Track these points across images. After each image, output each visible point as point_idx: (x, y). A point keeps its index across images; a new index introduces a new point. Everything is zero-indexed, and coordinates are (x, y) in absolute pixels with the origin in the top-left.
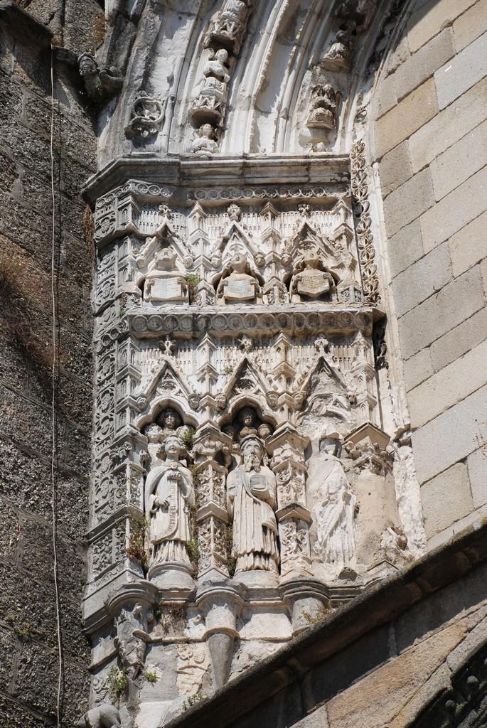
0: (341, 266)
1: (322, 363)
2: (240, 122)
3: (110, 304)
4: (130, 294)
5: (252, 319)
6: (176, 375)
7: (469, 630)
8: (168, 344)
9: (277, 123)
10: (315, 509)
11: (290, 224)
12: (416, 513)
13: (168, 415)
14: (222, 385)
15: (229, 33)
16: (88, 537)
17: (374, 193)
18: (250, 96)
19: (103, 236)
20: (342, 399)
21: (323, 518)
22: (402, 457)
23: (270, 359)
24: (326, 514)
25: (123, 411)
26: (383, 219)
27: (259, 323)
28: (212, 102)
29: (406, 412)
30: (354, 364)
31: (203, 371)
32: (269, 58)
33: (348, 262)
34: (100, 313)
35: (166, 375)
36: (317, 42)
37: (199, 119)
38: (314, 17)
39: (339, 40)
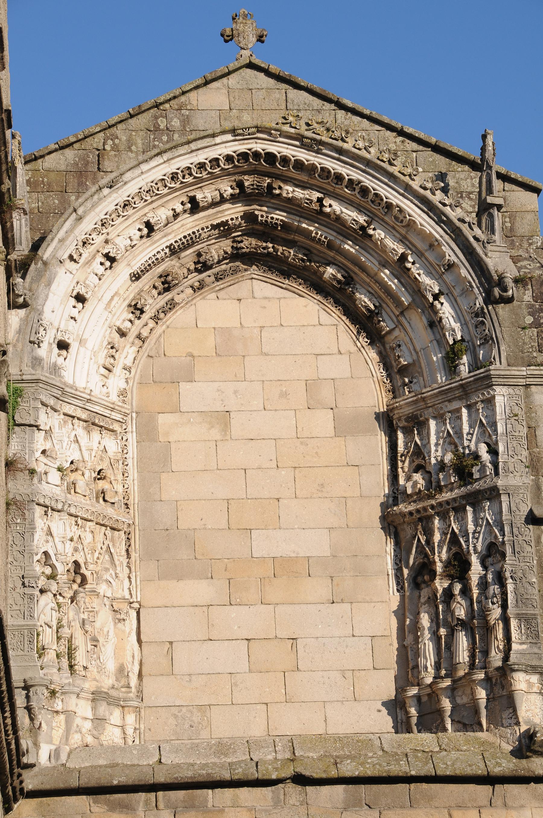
14: (69, 547)
36: (117, 315)
37: (63, 346)
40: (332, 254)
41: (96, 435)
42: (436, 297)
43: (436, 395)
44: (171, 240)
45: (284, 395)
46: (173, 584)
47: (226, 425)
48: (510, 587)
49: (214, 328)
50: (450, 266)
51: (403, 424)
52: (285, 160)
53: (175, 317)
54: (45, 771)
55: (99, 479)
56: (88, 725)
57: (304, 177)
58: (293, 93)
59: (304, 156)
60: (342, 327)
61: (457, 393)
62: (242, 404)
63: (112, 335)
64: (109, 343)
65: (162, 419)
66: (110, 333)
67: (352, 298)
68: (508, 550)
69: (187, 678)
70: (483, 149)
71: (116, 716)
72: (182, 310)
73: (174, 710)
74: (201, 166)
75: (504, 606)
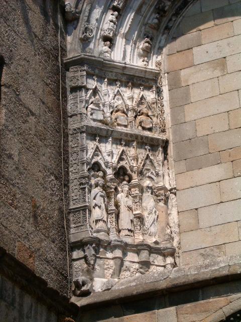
0: (154, 116)
1: (148, 157)
2: (120, 42)
3: (76, 115)
4: (84, 114)
5: (127, 134)
6: (100, 152)
7: (231, 302)
8: (98, 139)
9: (132, 46)
10: (145, 214)
11: (137, 93)
12: (176, 221)
13: (96, 167)
14: (115, 159)
15: (120, 6)
16: (70, 210)
17: (165, 86)
18: (124, 33)
19: (73, 85)
20: (154, 172)
21: (149, 219)
22: (172, 198)
23: (132, 151)
24: (149, 218)
25: (83, 164)
26: (168, 99)
27: (129, 136)
28: (112, 33)
29: (175, 183)
30: (158, 158)
31: (109, 152)
32: (132, 19)
33: (156, 115)
34: (71, 117)
35: (97, 151)
36: (148, 16)
37: (106, 39)
38: (149, 6)
39: (157, 18)
41: (137, 91)
46: (196, 172)
47: (223, 66)
49: (213, 10)
53: (187, 10)
55: (139, 116)
56: (137, 266)
62: (233, 51)
63: (147, 30)
64: (145, 35)
65: (183, 73)
66: (145, 28)
69: (208, 229)
71: (158, 260)
72: (192, 5)
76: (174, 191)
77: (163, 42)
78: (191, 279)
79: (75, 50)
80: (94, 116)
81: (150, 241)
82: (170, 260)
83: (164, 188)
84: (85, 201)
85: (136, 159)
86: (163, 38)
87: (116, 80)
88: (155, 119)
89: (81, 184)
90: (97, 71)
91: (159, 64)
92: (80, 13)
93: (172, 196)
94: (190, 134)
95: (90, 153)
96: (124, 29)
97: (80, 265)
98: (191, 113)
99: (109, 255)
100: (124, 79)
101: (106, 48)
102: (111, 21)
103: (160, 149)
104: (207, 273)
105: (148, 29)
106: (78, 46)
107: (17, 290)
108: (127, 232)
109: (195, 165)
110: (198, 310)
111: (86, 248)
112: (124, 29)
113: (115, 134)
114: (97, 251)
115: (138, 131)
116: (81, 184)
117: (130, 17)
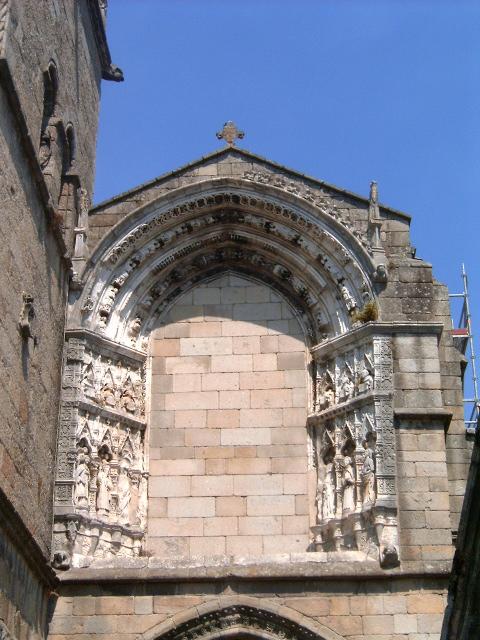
2: (115, 318)
5: (113, 415)
10: (121, 496)
12: (146, 506)
13: (83, 443)
21: (123, 502)
23: (115, 431)
37: (104, 314)
40: (277, 258)
41: (124, 370)
42: (340, 281)
43: (339, 341)
44: (176, 251)
45: (246, 345)
48: (378, 460)
49: (204, 305)
50: (349, 261)
51: (320, 361)
52: (245, 200)
54: (77, 571)
56: (109, 545)
57: (256, 210)
58: (255, 165)
59: (256, 196)
60: (285, 303)
61: (353, 339)
67: (291, 285)
68: (378, 436)
70: (371, 193)
71: (127, 541)
73: (167, 539)
74: (192, 205)
75: (374, 472)
76: (147, 476)
77: (151, 324)
78: (171, 574)
79: (75, 321)
80: (88, 393)
81: (123, 522)
82: (137, 543)
83: (137, 472)
84: (71, 476)
85: (117, 439)
86: (152, 321)
87: (108, 358)
88: (136, 401)
89: (69, 459)
90: (94, 347)
91: (145, 346)
92: (84, 284)
93: (144, 480)
94: (168, 423)
95: (80, 428)
96: (121, 306)
97: (60, 538)
98: (172, 403)
99: (88, 532)
100: (115, 357)
101: (102, 324)
102: (111, 298)
103: (139, 432)
104: (184, 571)
105: (140, 309)
106: (78, 318)
107: (26, 568)
108: (104, 512)
109: (170, 455)
110: (174, 603)
111: (69, 524)
112: (121, 306)
113: (103, 413)
114: (78, 527)
115: (122, 412)
116: (69, 459)
117: (128, 295)
